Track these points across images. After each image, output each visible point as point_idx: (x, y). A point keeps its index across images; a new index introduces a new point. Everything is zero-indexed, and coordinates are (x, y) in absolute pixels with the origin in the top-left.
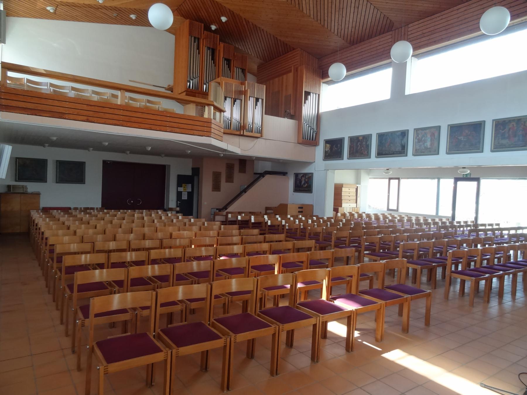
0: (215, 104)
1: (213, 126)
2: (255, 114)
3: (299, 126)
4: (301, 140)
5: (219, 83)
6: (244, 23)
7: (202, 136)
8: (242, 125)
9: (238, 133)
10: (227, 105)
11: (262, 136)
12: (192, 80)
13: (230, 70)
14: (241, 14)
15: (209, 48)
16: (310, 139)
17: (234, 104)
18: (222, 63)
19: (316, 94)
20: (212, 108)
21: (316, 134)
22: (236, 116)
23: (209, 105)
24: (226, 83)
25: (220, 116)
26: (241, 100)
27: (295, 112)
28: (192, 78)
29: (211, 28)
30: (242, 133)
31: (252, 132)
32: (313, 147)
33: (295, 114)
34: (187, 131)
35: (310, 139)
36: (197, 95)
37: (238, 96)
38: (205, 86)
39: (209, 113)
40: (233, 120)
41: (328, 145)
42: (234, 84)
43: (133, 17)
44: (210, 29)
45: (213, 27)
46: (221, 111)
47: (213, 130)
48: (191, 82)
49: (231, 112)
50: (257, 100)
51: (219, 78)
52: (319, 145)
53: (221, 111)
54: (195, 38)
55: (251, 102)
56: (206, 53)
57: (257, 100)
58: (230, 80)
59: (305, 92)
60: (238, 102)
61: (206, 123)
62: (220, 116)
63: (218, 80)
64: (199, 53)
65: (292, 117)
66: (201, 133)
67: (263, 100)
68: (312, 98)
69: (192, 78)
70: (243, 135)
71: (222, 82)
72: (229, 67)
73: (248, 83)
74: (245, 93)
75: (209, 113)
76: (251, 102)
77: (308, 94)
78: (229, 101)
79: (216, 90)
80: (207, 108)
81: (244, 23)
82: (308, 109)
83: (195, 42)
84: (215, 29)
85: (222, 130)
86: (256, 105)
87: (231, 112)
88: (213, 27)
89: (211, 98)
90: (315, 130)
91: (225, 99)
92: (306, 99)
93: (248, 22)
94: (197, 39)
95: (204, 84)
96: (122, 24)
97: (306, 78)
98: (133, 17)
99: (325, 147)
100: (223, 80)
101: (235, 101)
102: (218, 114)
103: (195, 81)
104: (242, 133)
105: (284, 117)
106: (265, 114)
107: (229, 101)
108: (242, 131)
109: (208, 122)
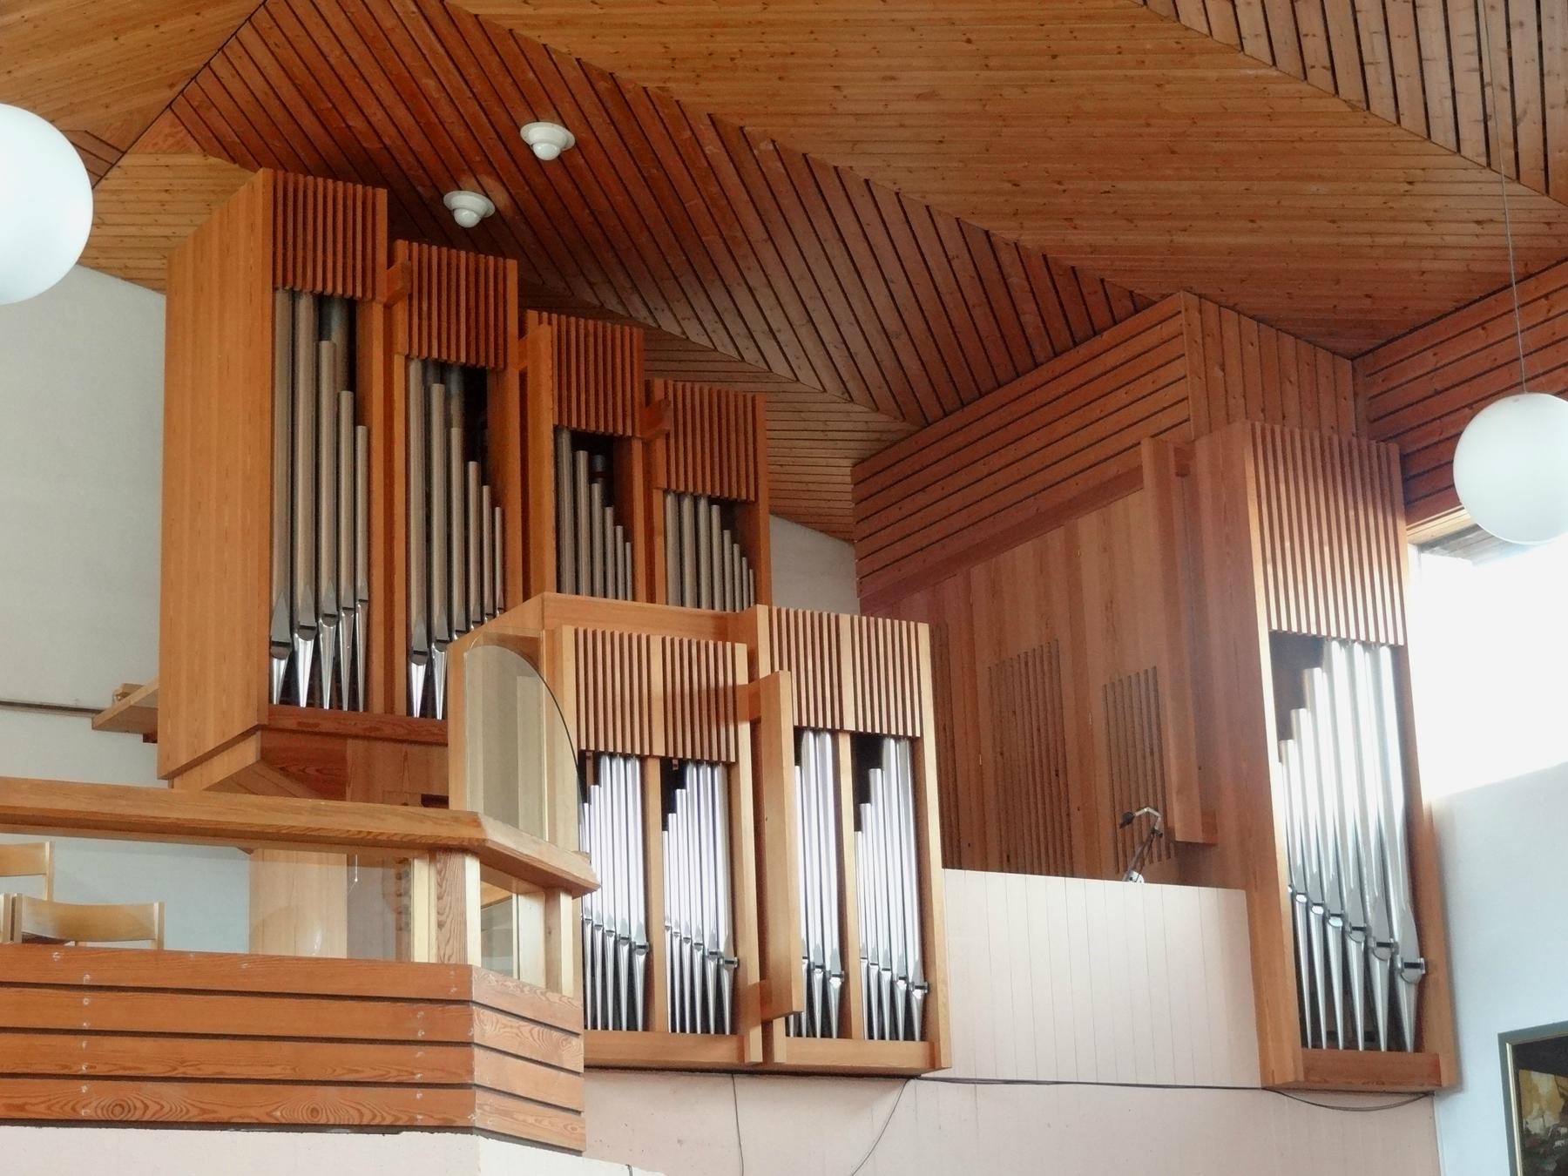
0: (499, 836)
1: (486, 1028)
2: (858, 869)
3: (1262, 936)
4: (1289, 1066)
5: (529, 651)
6: (713, 148)
7: (394, 1129)
8: (753, 976)
9: (721, 1052)
10: (603, 834)
11: (934, 1062)
12: (313, 633)
13: (623, 518)
14: (681, 90)
15: (439, 369)
16: (1371, 1036)
17: (668, 806)
18: (549, 470)
20: (472, 867)
21: (1421, 987)
22: (695, 906)
23: (437, 850)
24: (587, 646)
25: (550, 931)
26: (730, 768)
27: (1210, 820)
28: (306, 618)
29: (450, 213)
30: (755, 1054)
31: (844, 1032)
32: (1417, 1109)
33: (1210, 839)
34: (257, 1102)
35: (1371, 1036)
36: (341, 758)
37: (693, 742)
38: (418, 672)
39: (449, 922)
40: (666, 948)
41: (1544, 1083)
42: (656, 637)
44: (443, 229)
45: (468, 207)
46: (549, 885)
47: (485, 1069)
48: (305, 650)
49: (648, 874)
50: (867, 750)
51: (533, 602)
52: (1457, 1085)
53: (549, 885)
54: (322, 302)
55: (810, 784)
56: (420, 412)
57: (867, 750)
58: (619, 616)
59: (1275, 637)
60: (700, 785)
61: (422, 1012)
62: (550, 931)
63: (523, 619)
64: (358, 417)
65: (1185, 863)
66: (372, 1102)
67: (915, 743)
68: (1343, 691)
69: (306, 618)
70: (767, 1071)
71: (554, 635)
73: (782, 628)
74: (753, 705)
75: (449, 922)
76: (810, 784)
77: (1300, 653)
78: (620, 784)
79: (508, 716)
80: (422, 875)
81: (713, 148)
82: (1321, 788)
83: (321, 332)
84: (485, 222)
85: (574, 1054)
86: (862, 793)
87: (648, 874)
88: (468, 207)
89: (469, 788)
90: (1409, 952)
91: (588, 767)
92: (1292, 696)
93: (736, 140)
94: (341, 312)
95: (411, 654)
97: (1273, 530)
99: (1520, 1100)
100: (562, 618)
101: (673, 777)
102: (527, 912)
103: (337, 637)
104: (755, 1054)
105: (1119, 872)
106: (953, 860)
107: (620, 784)
108: (756, 1034)
109: (447, 997)
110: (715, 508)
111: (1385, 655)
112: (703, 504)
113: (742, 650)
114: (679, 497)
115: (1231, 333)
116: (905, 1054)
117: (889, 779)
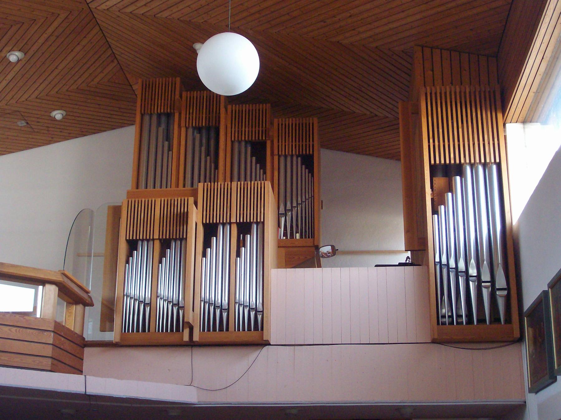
9: (174, 338)
15: (199, 129)
16: (481, 320)
17: (163, 254)
19: (485, 165)
21: (508, 298)
30: (186, 338)
32: (511, 350)
35: (481, 320)
40: (161, 303)
43: (58, 115)
57: (244, 229)
70: (191, 344)
72: (261, 161)
83: (159, 124)
91: (133, 245)
96: (66, 138)
98: (58, 115)
108: (186, 332)
110: (299, 159)
111: (494, 167)
112: (295, 158)
113: (191, 200)
114: (286, 156)
115: (437, 58)
116: (253, 336)
117: (251, 240)
